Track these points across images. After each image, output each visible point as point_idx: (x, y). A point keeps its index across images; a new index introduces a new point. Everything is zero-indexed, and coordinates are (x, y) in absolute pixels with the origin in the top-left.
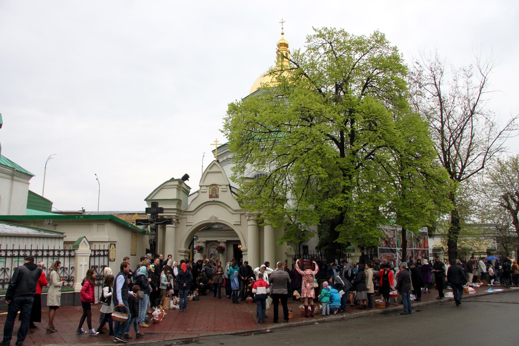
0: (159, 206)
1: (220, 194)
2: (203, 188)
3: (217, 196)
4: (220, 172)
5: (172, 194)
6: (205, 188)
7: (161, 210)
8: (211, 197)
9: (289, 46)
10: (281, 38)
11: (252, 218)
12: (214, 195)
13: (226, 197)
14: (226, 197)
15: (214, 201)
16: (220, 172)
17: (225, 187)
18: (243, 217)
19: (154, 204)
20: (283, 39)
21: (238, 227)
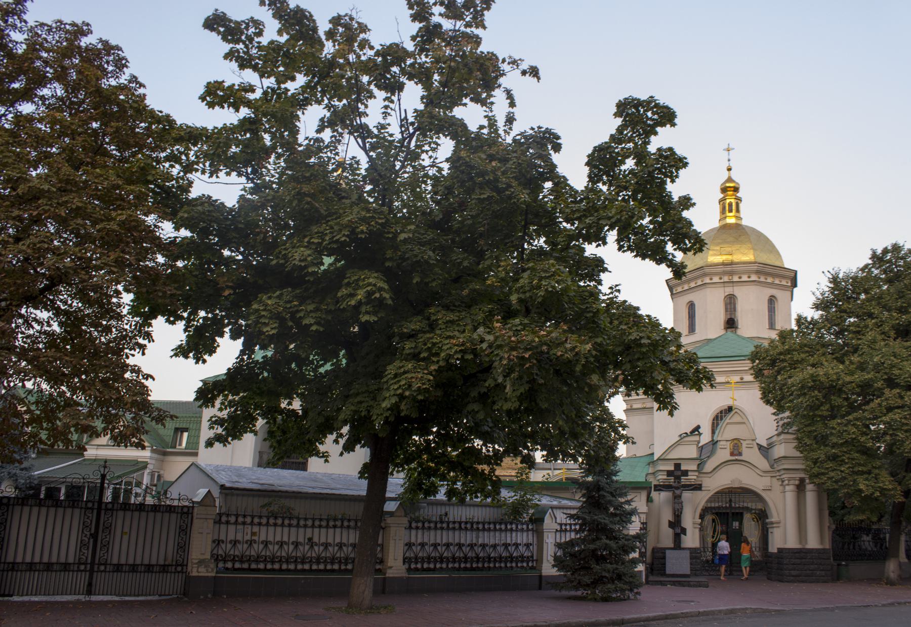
0: (683, 468)
1: (744, 450)
2: (721, 443)
3: (740, 454)
4: (744, 423)
5: (690, 451)
6: (724, 443)
7: (685, 473)
8: (732, 454)
9: (741, 190)
10: (726, 178)
11: (792, 482)
12: (736, 452)
13: (751, 454)
14: (751, 454)
15: (736, 460)
16: (744, 423)
17: (750, 442)
18: (774, 479)
19: (677, 466)
20: (730, 180)
21: (768, 492)
